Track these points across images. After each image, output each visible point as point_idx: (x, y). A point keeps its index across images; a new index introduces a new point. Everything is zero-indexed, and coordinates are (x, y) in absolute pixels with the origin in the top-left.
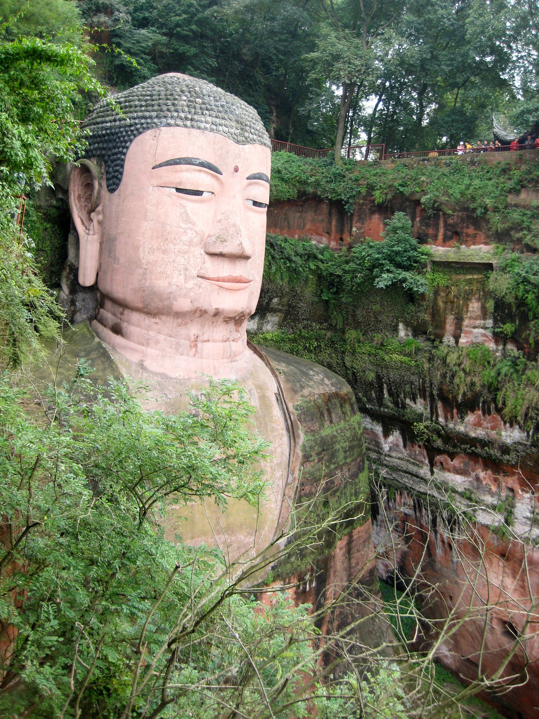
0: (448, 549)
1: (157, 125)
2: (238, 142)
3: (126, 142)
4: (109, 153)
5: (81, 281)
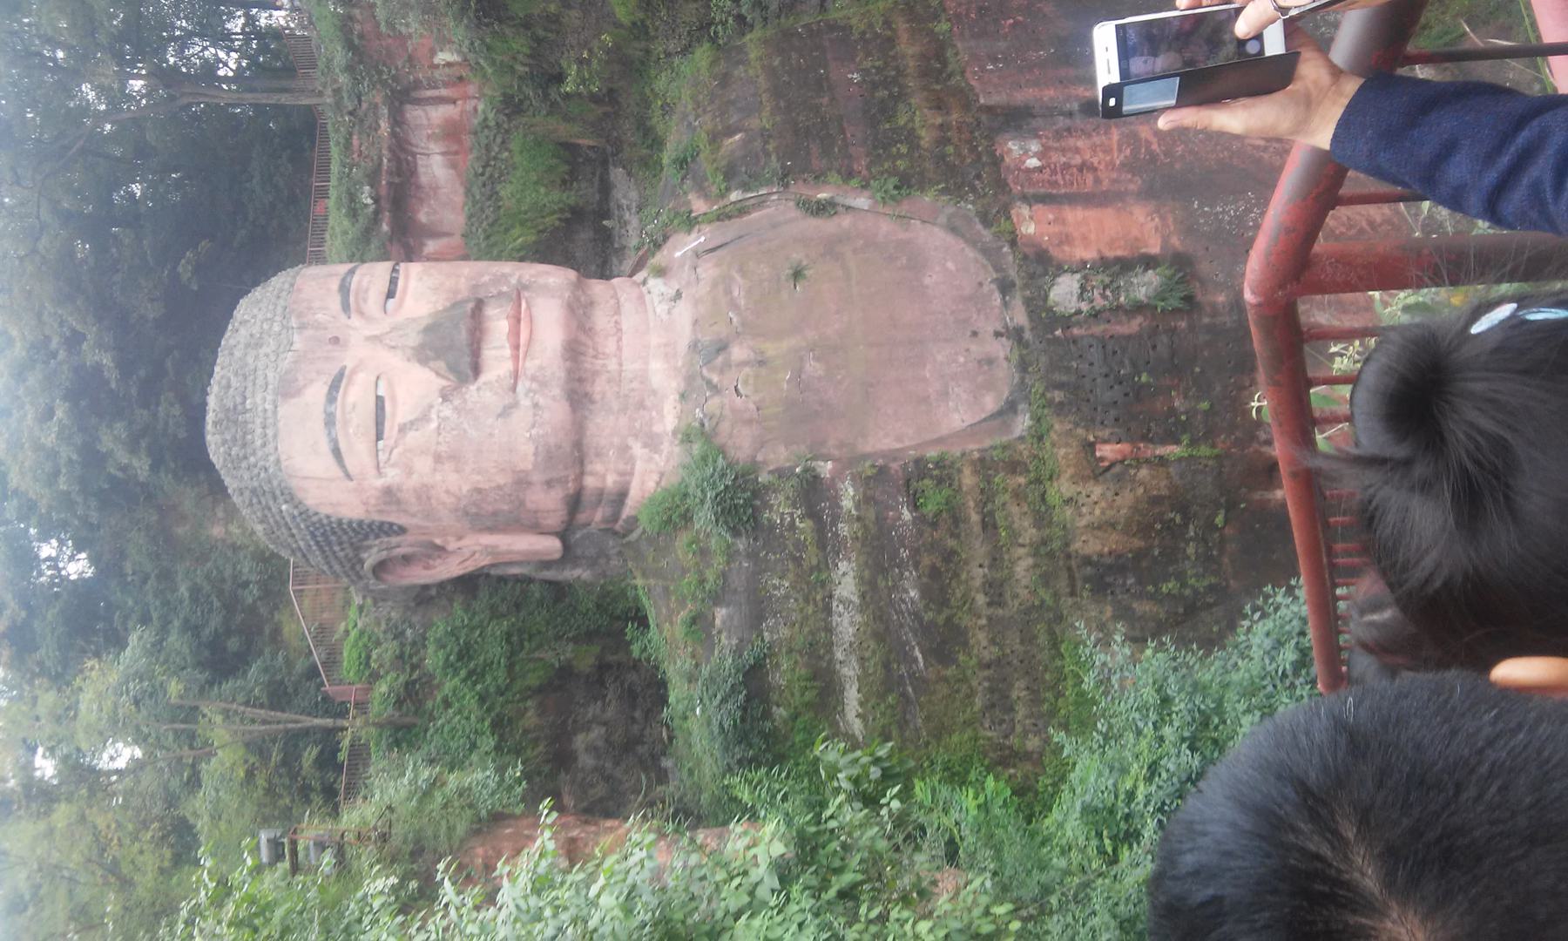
5: (557, 556)
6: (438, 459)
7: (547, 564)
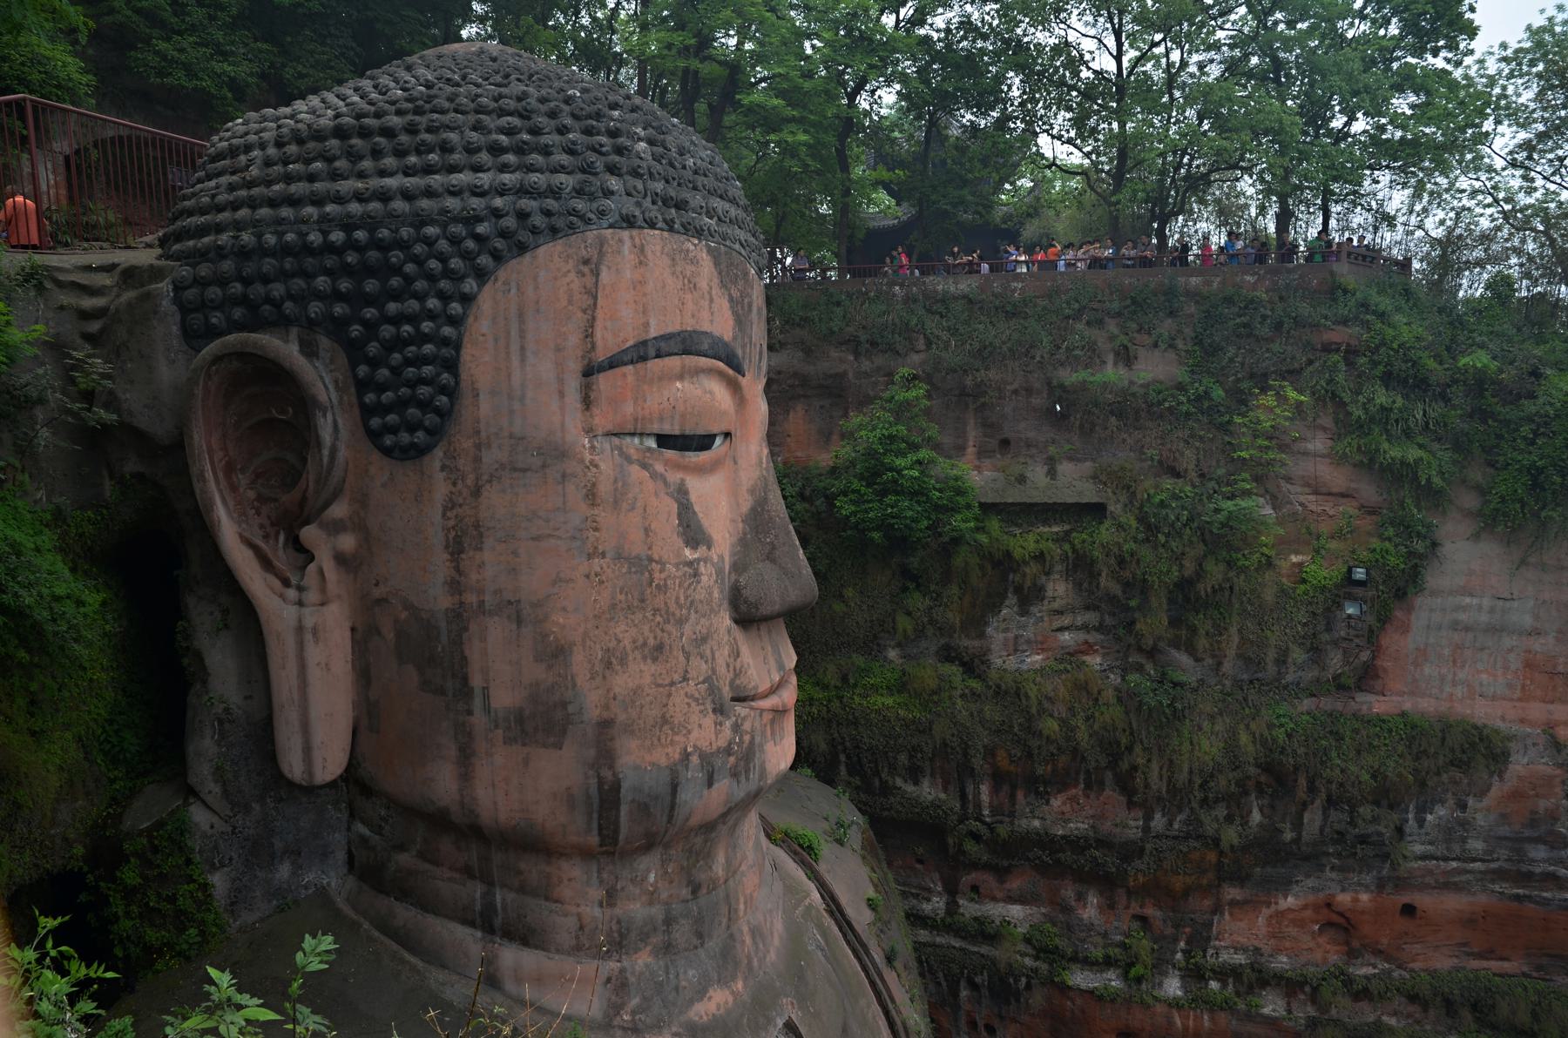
1: (582, 217)
4: (370, 313)
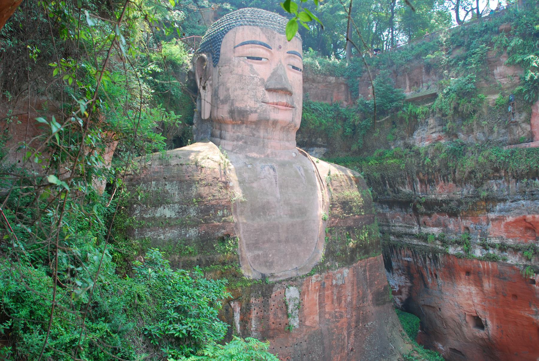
0: (435, 277)
2: (280, 33)
3: (220, 39)
5: (203, 118)
6: (241, 76)
7: (200, 113)
